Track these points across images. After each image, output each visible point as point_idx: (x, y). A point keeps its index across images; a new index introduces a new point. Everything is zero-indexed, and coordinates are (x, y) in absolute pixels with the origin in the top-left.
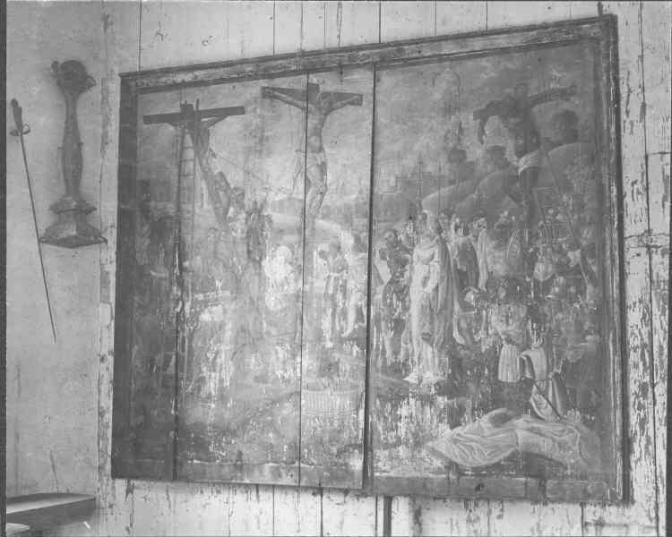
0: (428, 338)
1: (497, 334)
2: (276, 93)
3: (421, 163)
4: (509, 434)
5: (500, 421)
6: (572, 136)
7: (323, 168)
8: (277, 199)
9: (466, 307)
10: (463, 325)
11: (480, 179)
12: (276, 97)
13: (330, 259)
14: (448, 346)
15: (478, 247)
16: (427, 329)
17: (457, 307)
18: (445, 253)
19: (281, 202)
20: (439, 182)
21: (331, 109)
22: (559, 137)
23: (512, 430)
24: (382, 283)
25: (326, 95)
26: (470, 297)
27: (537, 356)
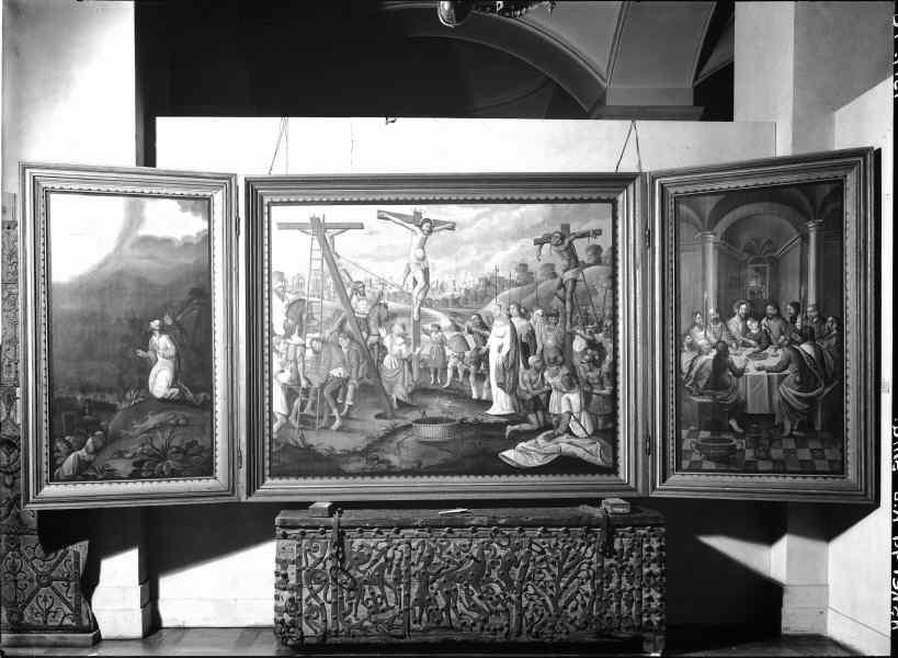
0: (501, 385)
1: (548, 384)
2: (389, 217)
3: (497, 270)
4: (555, 446)
5: (549, 438)
6: (598, 262)
7: (426, 272)
8: (391, 291)
9: (527, 366)
10: (526, 377)
11: (537, 284)
12: (387, 219)
13: (433, 334)
14: (512, 390)
15: (536, 328)
16: (501, 380)
17: (521, 365)
18: (513, 329)
19: (395, 294)
20: (512, 284)
21: (430, 232)
22: (591, 262)
23: (557, 443)
24: (469, 348)
25: (428, 220)
26: (531, 360)
27: (575, 398)
